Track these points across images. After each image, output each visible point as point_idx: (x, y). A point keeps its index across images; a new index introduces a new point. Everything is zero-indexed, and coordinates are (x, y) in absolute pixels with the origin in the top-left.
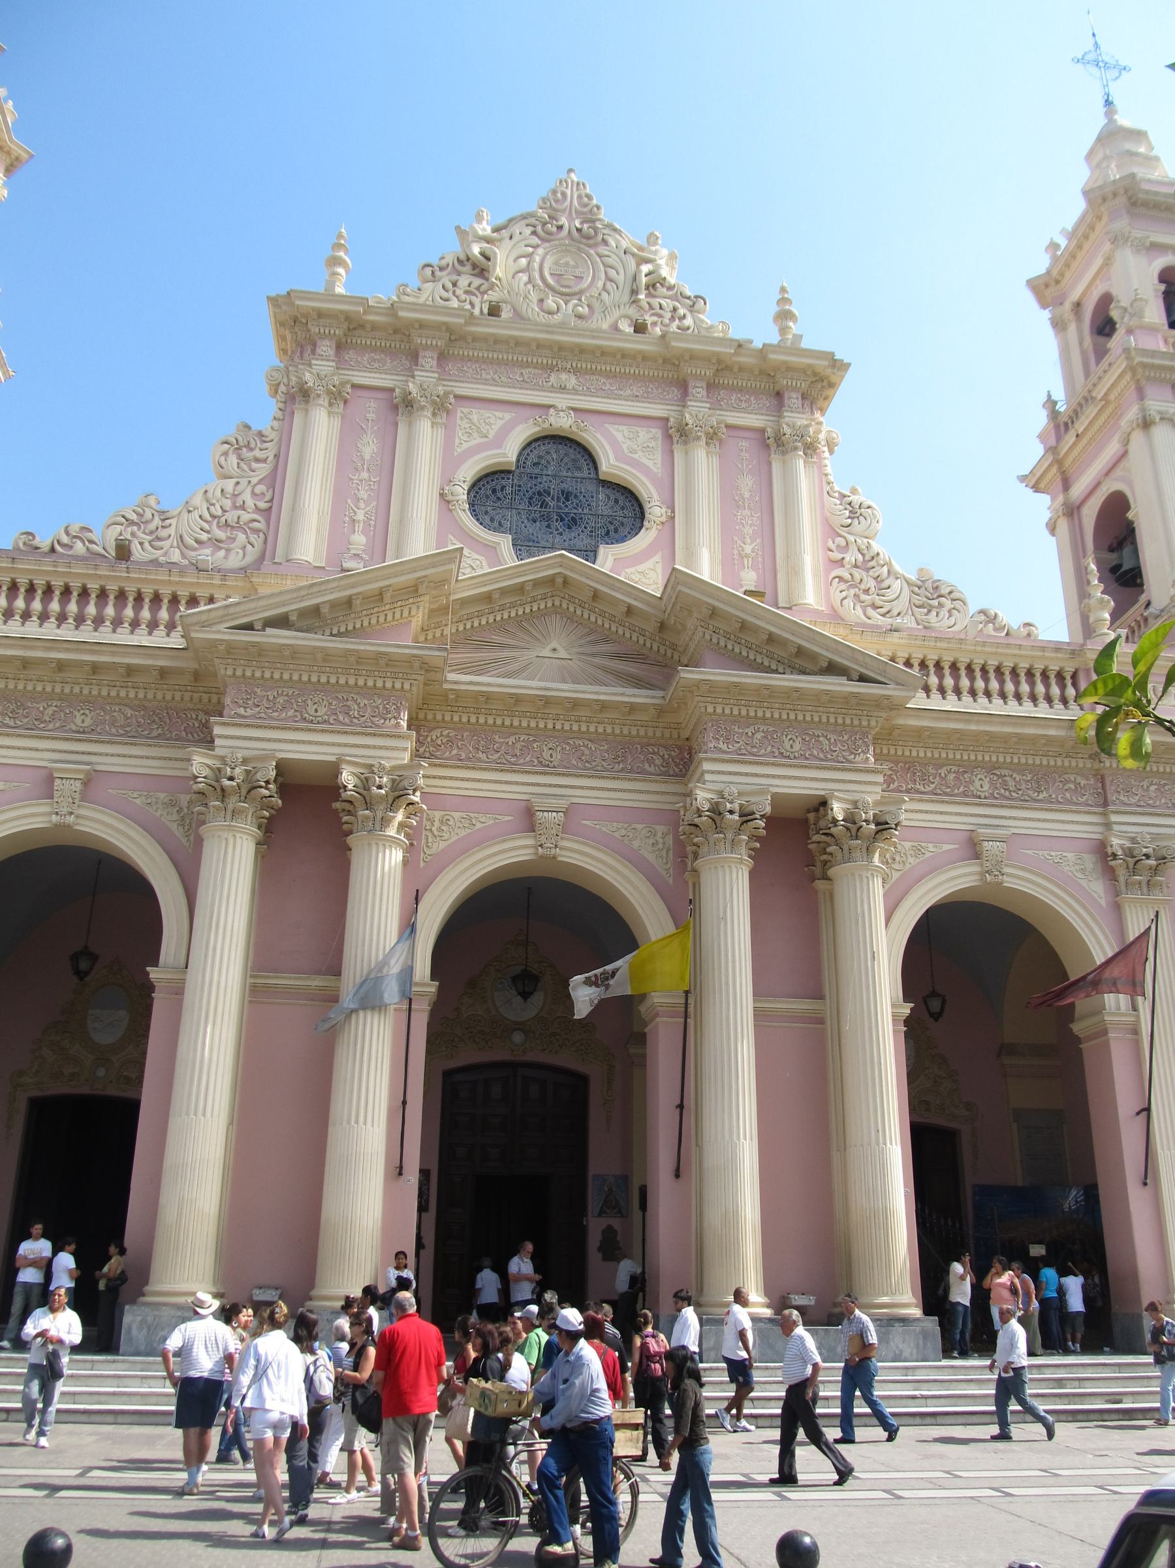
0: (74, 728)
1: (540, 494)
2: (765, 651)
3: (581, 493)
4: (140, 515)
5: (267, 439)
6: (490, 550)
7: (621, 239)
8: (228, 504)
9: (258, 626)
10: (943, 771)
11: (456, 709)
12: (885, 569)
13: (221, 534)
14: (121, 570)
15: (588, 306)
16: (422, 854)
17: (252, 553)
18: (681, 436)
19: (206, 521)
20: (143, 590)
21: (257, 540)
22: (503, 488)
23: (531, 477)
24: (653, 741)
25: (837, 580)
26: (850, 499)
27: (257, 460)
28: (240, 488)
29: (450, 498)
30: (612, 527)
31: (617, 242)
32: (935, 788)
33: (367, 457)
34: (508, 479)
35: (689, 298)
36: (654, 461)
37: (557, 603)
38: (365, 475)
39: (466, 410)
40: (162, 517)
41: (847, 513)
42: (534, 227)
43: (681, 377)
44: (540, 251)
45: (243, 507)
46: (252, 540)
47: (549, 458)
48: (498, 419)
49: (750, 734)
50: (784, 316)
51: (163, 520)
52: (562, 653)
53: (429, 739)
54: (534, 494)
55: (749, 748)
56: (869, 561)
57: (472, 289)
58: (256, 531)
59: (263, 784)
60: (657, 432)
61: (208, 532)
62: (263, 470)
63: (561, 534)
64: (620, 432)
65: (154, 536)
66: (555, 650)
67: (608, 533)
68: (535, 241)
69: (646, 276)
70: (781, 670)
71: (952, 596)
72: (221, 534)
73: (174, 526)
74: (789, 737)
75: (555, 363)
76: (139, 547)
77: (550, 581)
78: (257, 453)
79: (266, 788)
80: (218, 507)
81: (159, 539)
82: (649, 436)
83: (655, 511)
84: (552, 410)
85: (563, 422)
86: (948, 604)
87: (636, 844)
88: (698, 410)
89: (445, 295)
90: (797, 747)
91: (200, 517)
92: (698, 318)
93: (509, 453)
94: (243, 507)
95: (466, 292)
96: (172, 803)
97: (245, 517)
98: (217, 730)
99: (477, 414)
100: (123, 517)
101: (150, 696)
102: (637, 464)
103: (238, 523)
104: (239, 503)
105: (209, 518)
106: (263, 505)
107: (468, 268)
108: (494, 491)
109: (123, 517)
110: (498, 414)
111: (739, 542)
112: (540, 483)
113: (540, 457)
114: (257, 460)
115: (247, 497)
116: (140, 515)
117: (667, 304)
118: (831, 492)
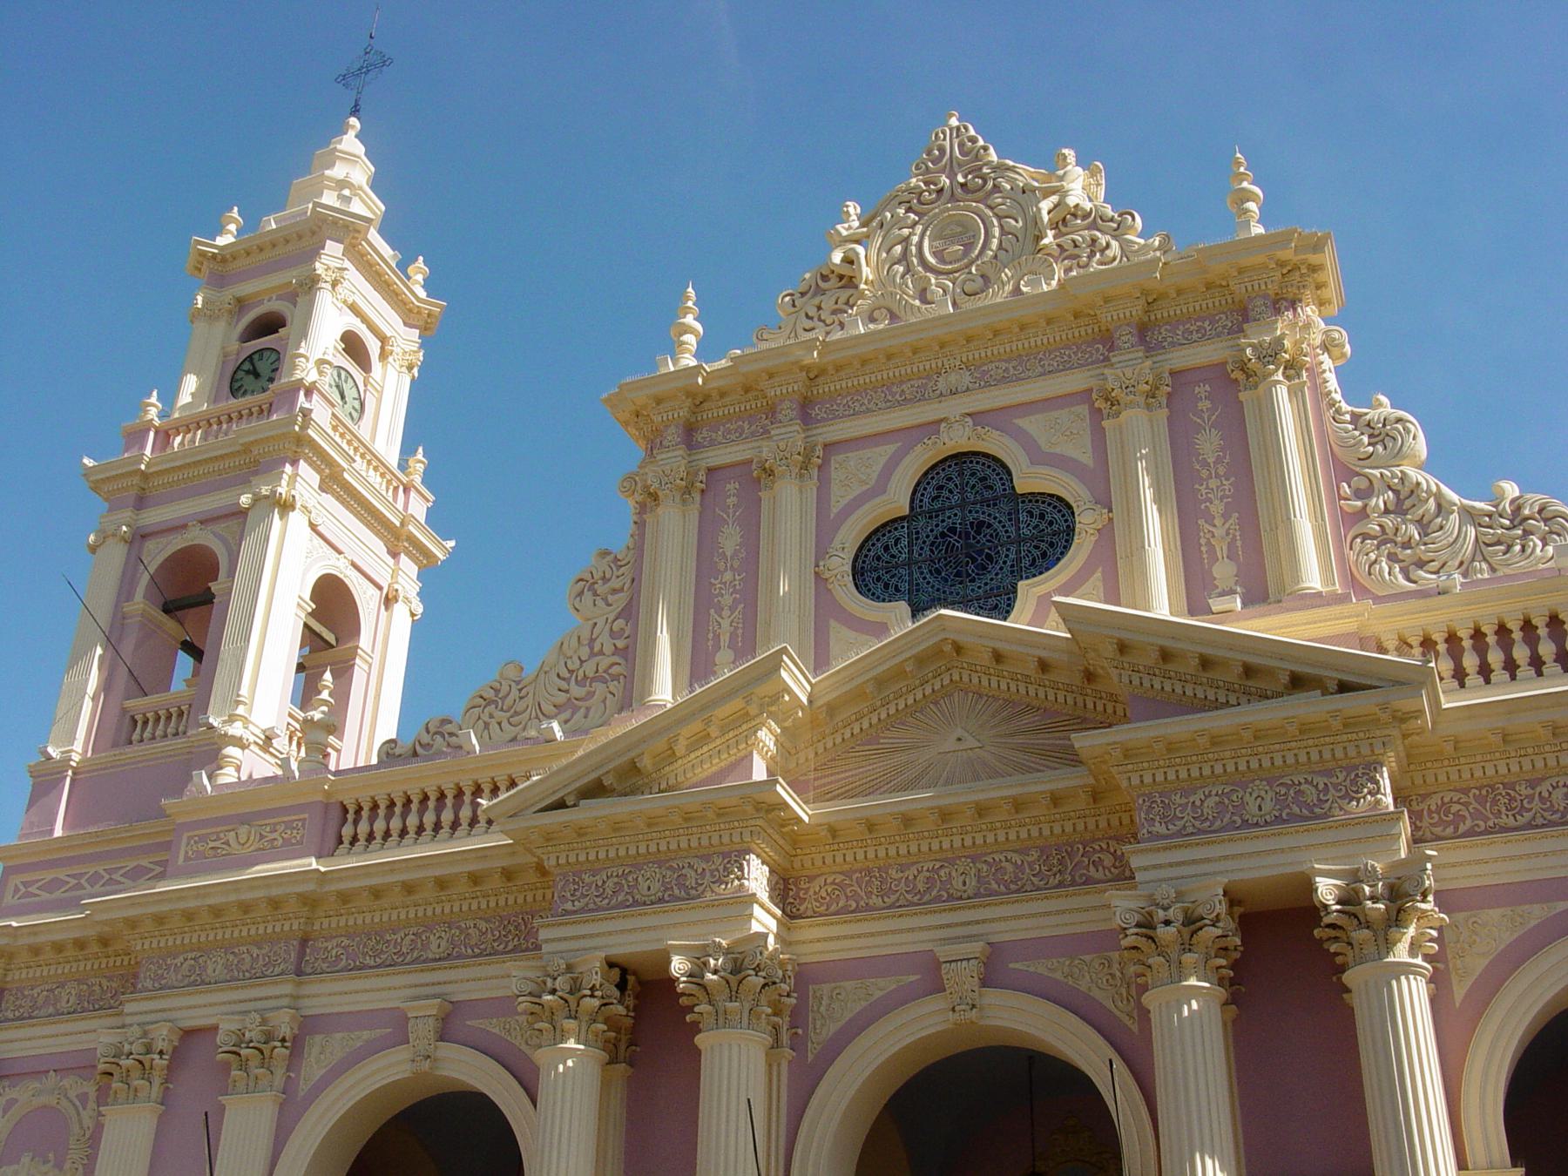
0: (431, 956)
1: (943, 535)
2: (1205, 680)
3: (995, 518)
4: (497, 691)
5: (622, 563)
7: (1017, 176)
8: (584, 652)
9: (570, 801)
10: (1544, 788)
11: (836, 847)
12: (1432, 503)
13: (577, 691)
15: (982, 276)
16: (809, 1044)
18: (1112, 405)
19: (564, 679)
20: (480, 781)
22: (897, 541)
23: (931, 517)
24: (1099, 835)
25: (1359, 540)
26: (1368, 417)
27: (614, 591)
28: (596, 631)
29: (827, 575)
30: (1037, 553)
31: (1012, 181)
32: (1534, 818)
33: (729, 554)
34: (903, 527)
35: (1112, 220)
36: (1083, 454)
37: (956, 677)
38: (728, 576)
39: (841, 457)
40: (520, 687)
41: (1365, 439)
42: (909, 202)
43: (1103, 328)
44: (919, 229)
45: (601, 653)
46: (612, 688)
47: (951, 485)
49: (1198, 803)
51: (520, 690)
52: (971, 742)
53: (811, 892)
54: (936, 538)
55: (1197, 823)
57: (840, 305)
58: (615, 678)
59: (588, 992)
60: (1083, 410)
61: (567, 691)
62: (620, 601)
63: (973, 580)
64: (1031, 424)
65: (512, 710)
66: (959, 739)
67: (1033, 564)
69: (1049, 213)
70: (1233, 701)
71: (1546, 514)
72: (577, 691)
73: (531, 695)
74: (1254, 795)
75: (940, 365)
76: (497, 726)
77: (936, 653)
78: (615, 584)
79: (592, 996)
80: (575, 659)
81: (517, 713)
84: (943, 425)
85: (959, 439)
87: (1083, 985)
88: (1130, 366)
90: (1267, 806)
91: (558, 675)
92: (1126, 239)
94: (601, 653)
95: (834, 312)
97: (605, 662)
98: (543, 934)
99: (853, 458)
100: (482, 697)
101: (501, 903)
103: (597, 671)
104: (596, 649)
105: (567, 675)
106: (620, 644)
107: (834, 282)
108: (886, 548)
109: (482, 697)
110: (878, 450)
111: (1207, 526)
112: (943, 521)
113: (940, 488)
114: (614, 591)
116: (497, 691)
118: (1337, 416)
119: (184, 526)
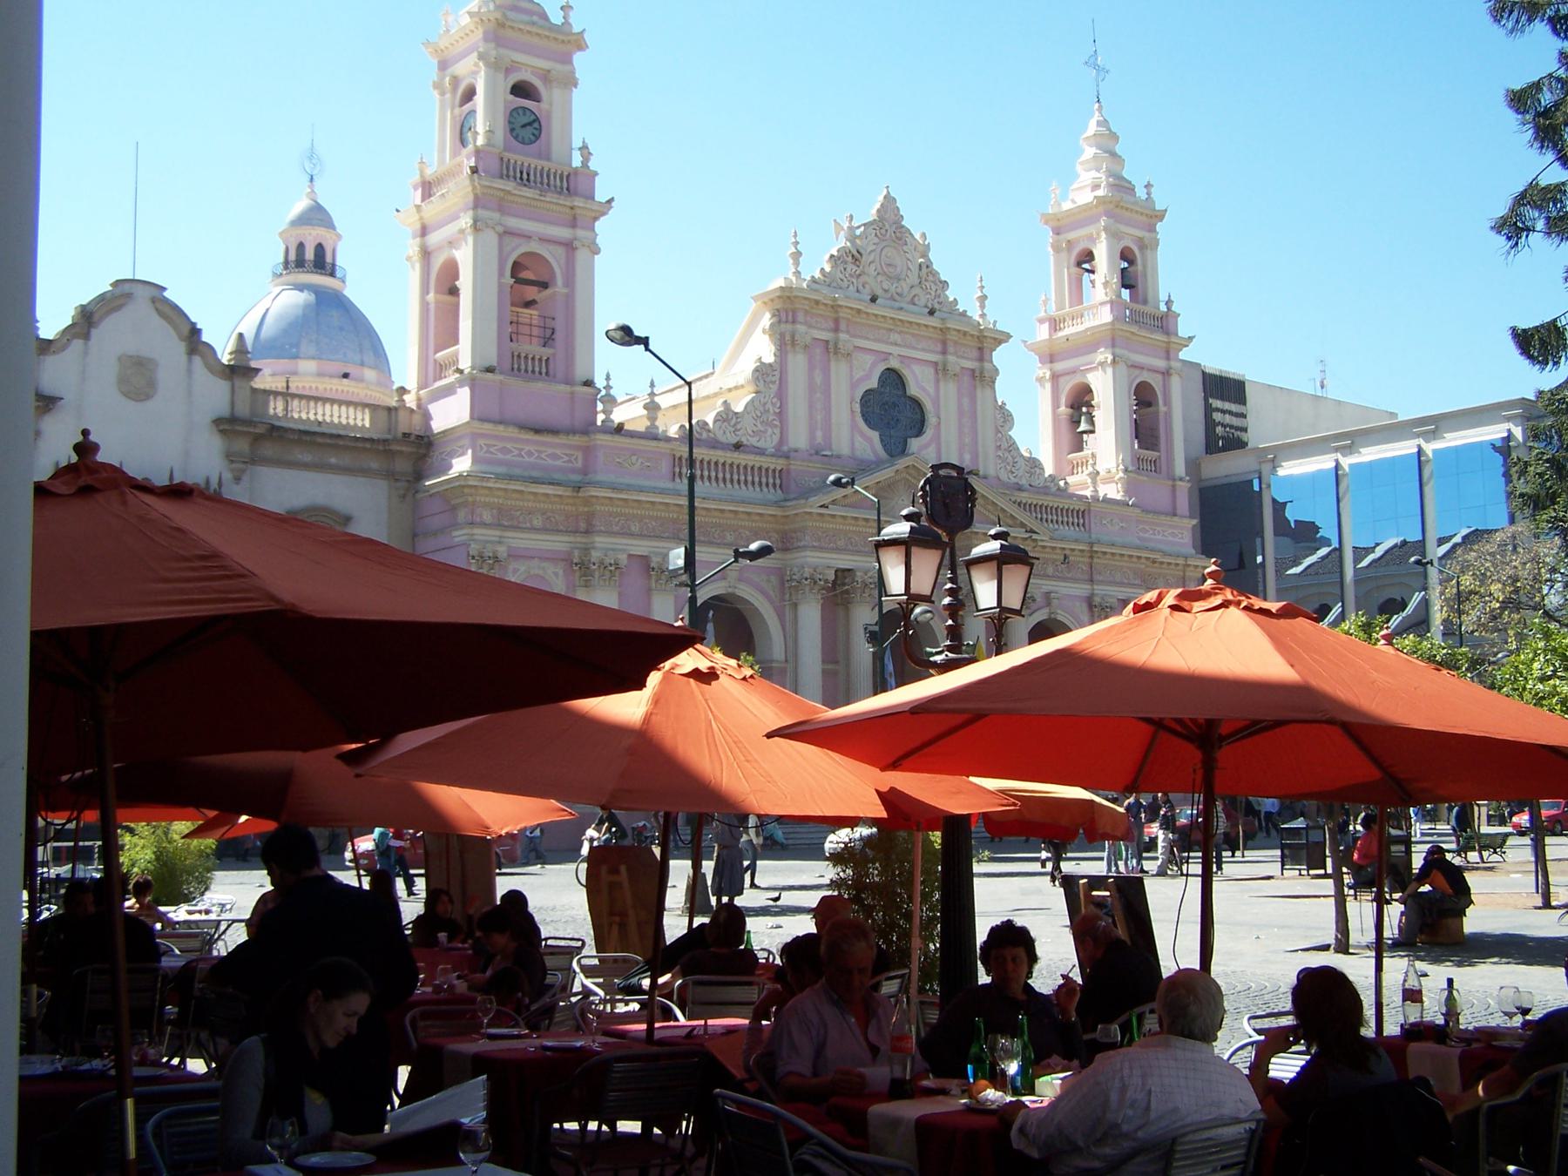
6: (869, 440)
8: (762, 409)
13: (760, 427)
14: (736, 455)
17: (776, 439)
21: (777, 431)
36: (931, 390)
48: (869, 359)
50: (983, 299)
56: (1012, 447)
60: (932, 370)
62: (774, 388)
64: (917, 369)
68: (876, 240)
72: (760, 427)
82: (929, 372)
83: (931, 419)
86: (1038, 471)
89: (842, 276)
93: (873, 383)
96: (769, 581)
97: (771, 418)
102: (924, 389)
106: (777, 411)
115: (769, 406)
117: (934, 288)
119: (530, 237)
